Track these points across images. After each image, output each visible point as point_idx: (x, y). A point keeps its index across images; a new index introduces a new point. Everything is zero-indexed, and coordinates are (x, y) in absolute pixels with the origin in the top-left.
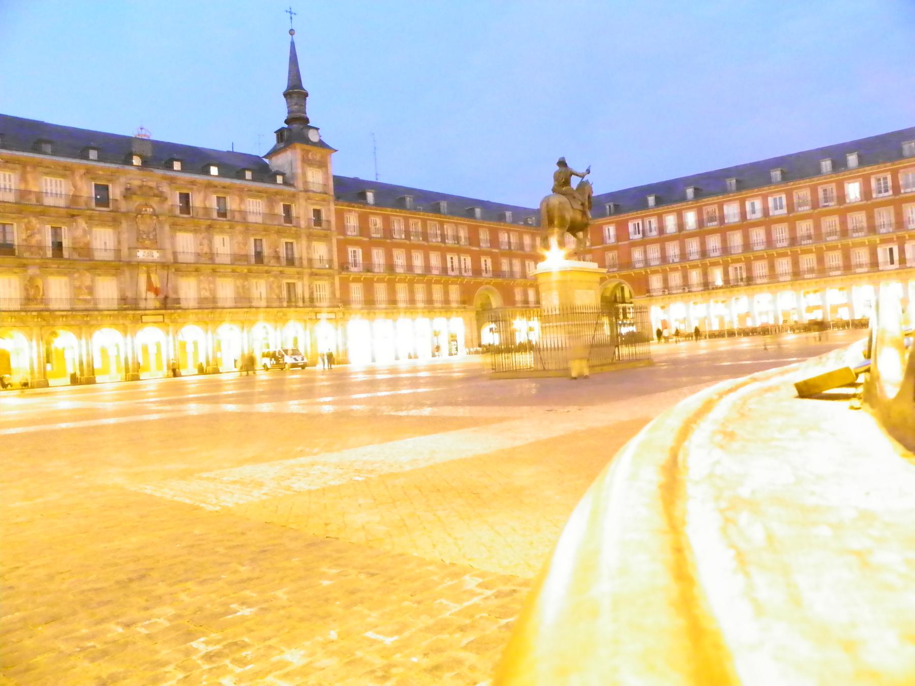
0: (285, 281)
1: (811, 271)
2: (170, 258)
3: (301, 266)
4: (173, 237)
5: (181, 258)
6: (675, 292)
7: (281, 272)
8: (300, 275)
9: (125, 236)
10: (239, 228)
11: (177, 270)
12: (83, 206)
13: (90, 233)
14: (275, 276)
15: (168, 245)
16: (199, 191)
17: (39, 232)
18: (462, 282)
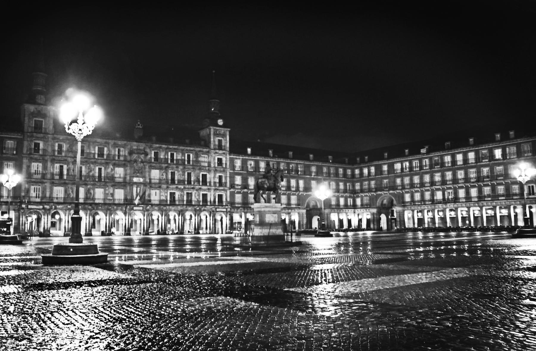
0: (202, 193)
1: (489, 196)
2: (148, 181)
3: (210, 185)
4: (150, 172)
5: (153, 181)
6: (427, 203)
7: (200, 189)
8: (209, 190)
9: (128, 171)
10: (181, 167)
11: (151, 187)
12: (112, 158)
13: (114, 169)
14: (197, 190)
15: (147, 175)
16: (163, 151)
17: (94, 170)
18: (298, 194)
